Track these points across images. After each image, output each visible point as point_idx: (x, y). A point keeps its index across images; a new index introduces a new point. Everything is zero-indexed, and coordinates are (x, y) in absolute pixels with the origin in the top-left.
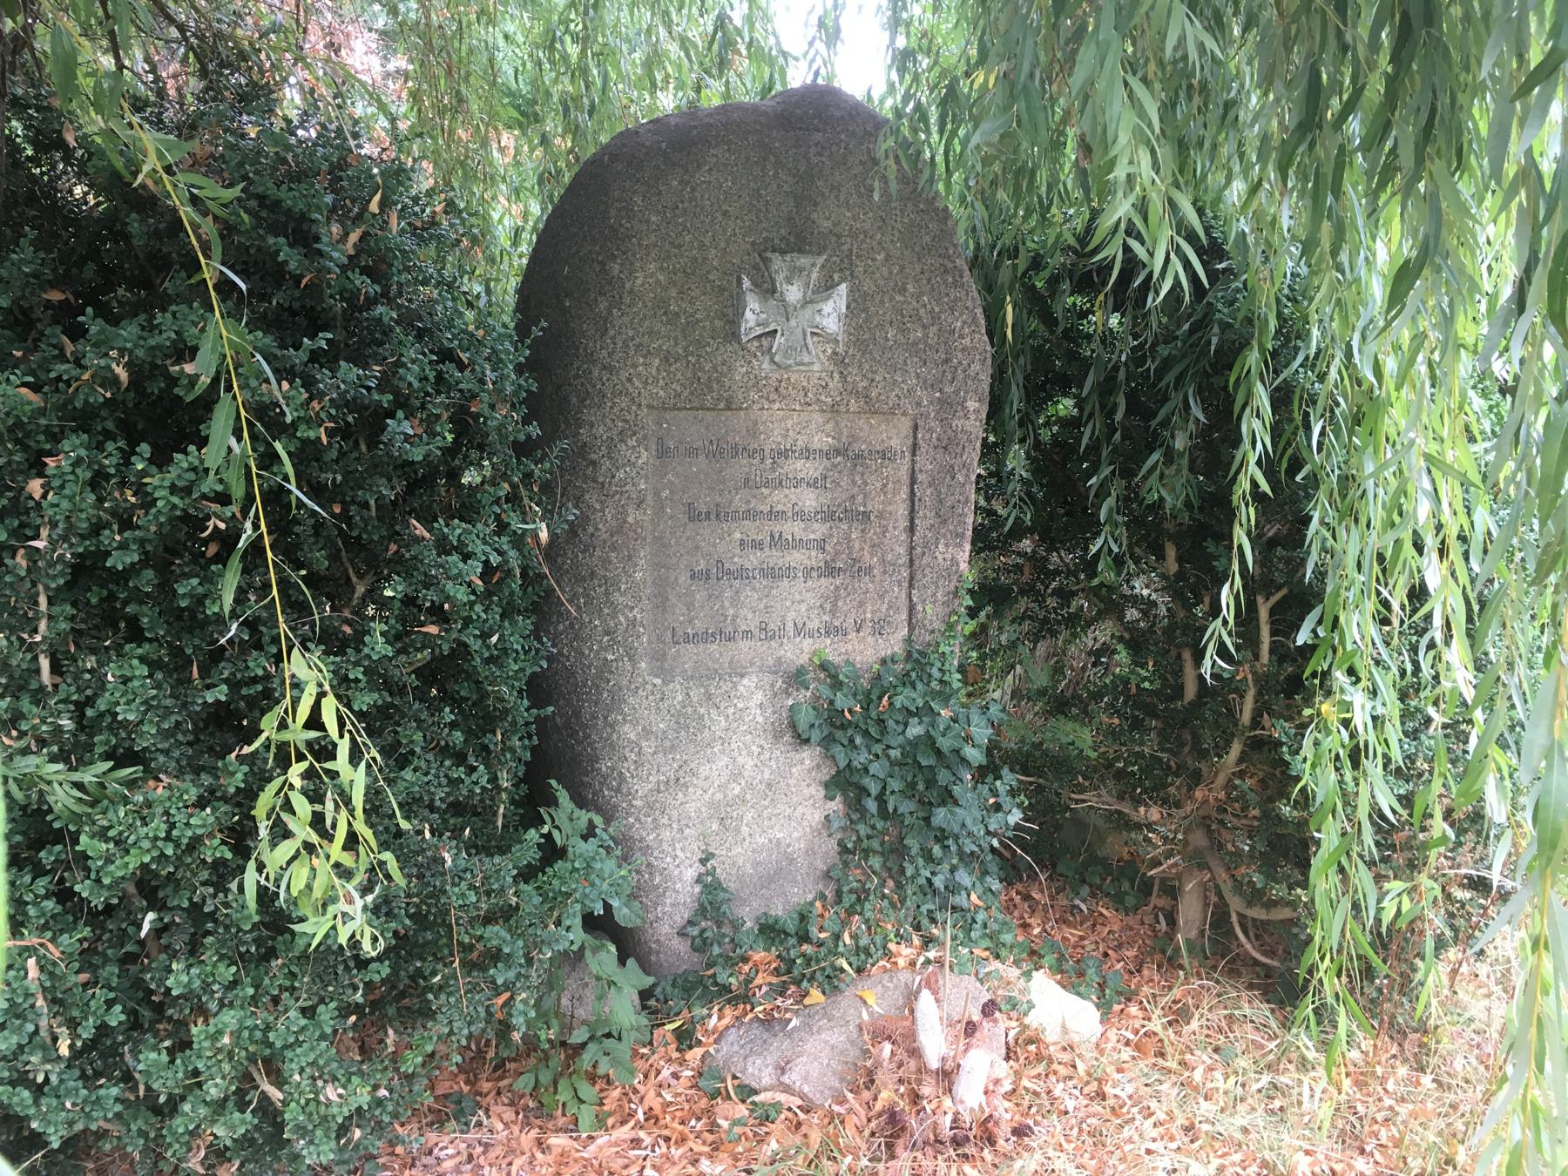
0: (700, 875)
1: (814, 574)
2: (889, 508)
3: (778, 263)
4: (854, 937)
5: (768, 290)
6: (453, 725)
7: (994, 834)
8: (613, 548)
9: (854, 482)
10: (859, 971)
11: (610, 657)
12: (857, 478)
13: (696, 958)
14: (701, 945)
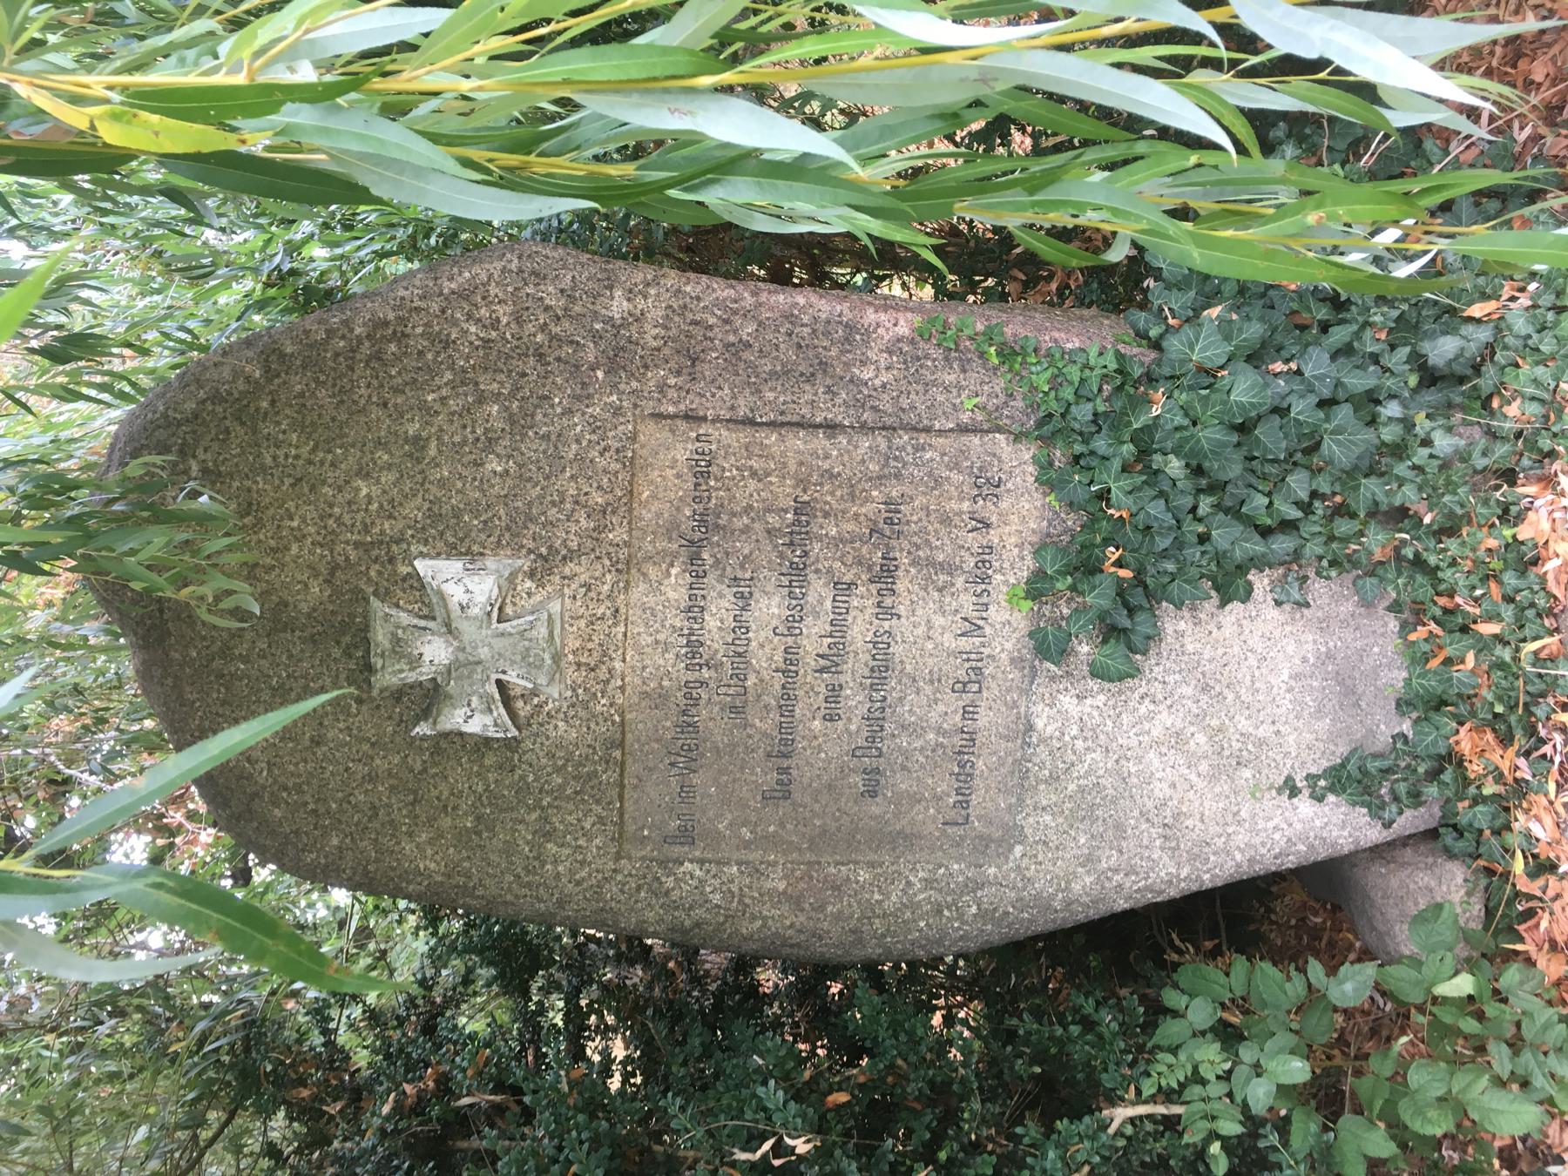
0: (1312, 796)
1: (888, 602)
2: (792, 467)
3: (390, 676)
5: (429, 697)
9: (746, 530)
11: (974, 910)
12: (739, 523)
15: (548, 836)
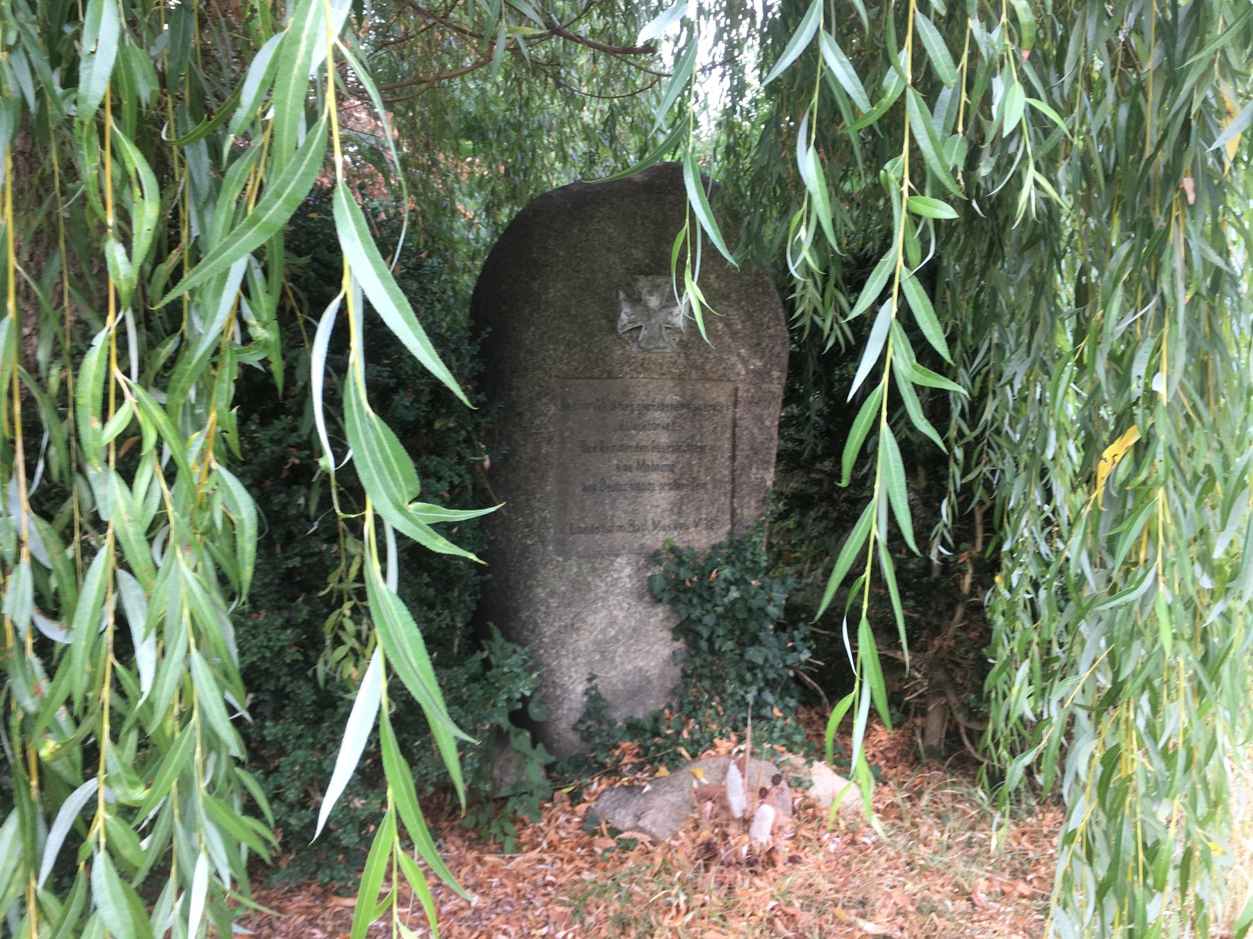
4: (691, 733)
5: (636, 300)
6: (428, 585)
7: (789, 667)
8: (533, 470)
10: (694, 756)
13: (584, 745)
14: (587, 737)
15: (568, 346)
